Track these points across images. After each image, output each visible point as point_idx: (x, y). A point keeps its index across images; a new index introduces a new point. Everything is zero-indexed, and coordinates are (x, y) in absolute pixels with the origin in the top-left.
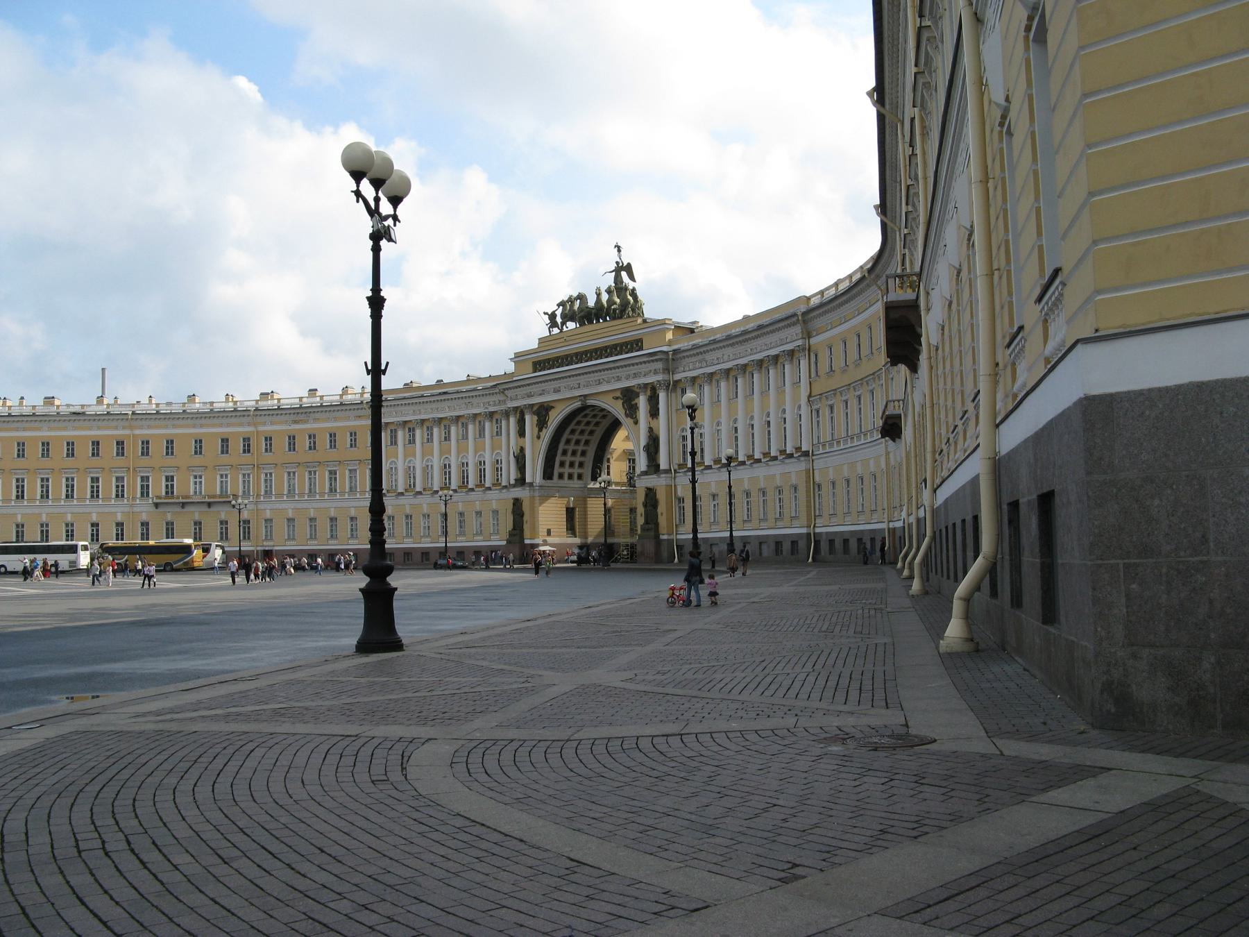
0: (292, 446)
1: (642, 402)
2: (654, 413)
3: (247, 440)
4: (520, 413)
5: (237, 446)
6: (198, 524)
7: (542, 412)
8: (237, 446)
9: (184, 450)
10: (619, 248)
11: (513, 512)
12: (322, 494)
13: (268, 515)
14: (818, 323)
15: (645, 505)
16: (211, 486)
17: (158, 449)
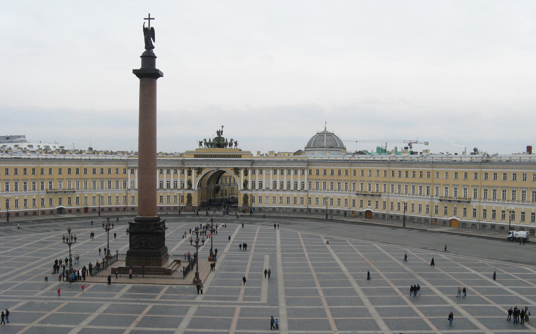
0: (94, 172)
1: (242, 172)
2: (246, 174)
3: (77, 169)
4: (190, 168)
5: (74, 171)
6: (60, 199)
7: (199, 170)
8: (74, 171)
9: (55, 172)
10: (223, 127)
12: (113, 188)
13: (86, 195)
14: (312, 164)
16: (64, 185)
17: (46, 172)
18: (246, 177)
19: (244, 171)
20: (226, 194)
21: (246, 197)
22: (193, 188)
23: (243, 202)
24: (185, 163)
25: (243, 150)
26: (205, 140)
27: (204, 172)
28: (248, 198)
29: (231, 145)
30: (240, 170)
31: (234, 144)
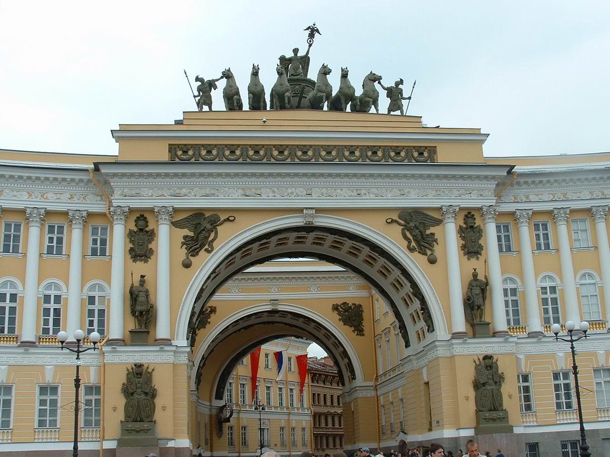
1: (449, 236)
7: (199, 228)
10: (313, 31)
11: (127, 391)
15: (477, 385)
18: (474, 263)
19: (461, 231)
20: (245, 443)
21: (488, 376)
22: (162, 330)
23: (472, 407)
24: (114, 182)
25: (429, 122)
26: (227, 75)
27: (228, 240)
28: (498, 380)
29: (363, 105)
30: (439, 222)
31: (384, 102)
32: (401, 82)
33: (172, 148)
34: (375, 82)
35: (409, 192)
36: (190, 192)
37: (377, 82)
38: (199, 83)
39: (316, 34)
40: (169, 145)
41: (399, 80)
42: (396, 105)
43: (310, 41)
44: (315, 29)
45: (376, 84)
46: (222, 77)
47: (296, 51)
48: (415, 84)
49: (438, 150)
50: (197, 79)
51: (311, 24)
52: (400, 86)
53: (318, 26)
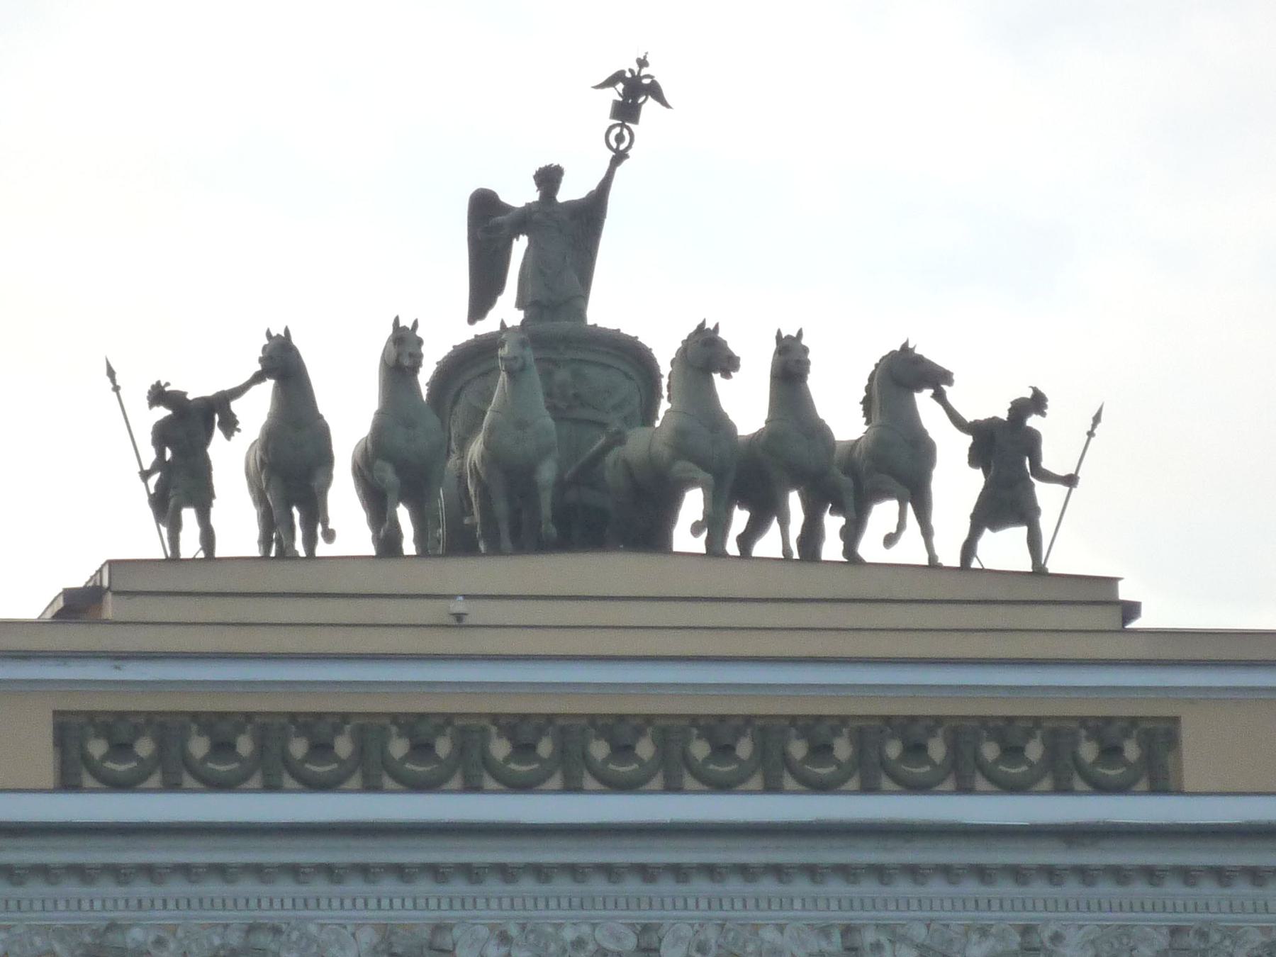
10: (633, 93)
26: (282, 363)
31: (956, 483)
32: (1037, 402)
33: (69, 732)
34: (919, 389)
35: (1057, 938)
36: (160, 942)
37: (928, 392)
38: (162, 412)
39: (649, 106)
40: (55, 712)
41: (1028, 394)
42: (1006, 502)
43: (620, 138)
44: (646, 81)
45: (924, 400)
46: (258, 378)
47: (549, 178)
48: (1097, 419)
49: (1188, 735)
50: (159, 395)
51: (628, 64)
52: (1033, 421)
53: (656, 71)
